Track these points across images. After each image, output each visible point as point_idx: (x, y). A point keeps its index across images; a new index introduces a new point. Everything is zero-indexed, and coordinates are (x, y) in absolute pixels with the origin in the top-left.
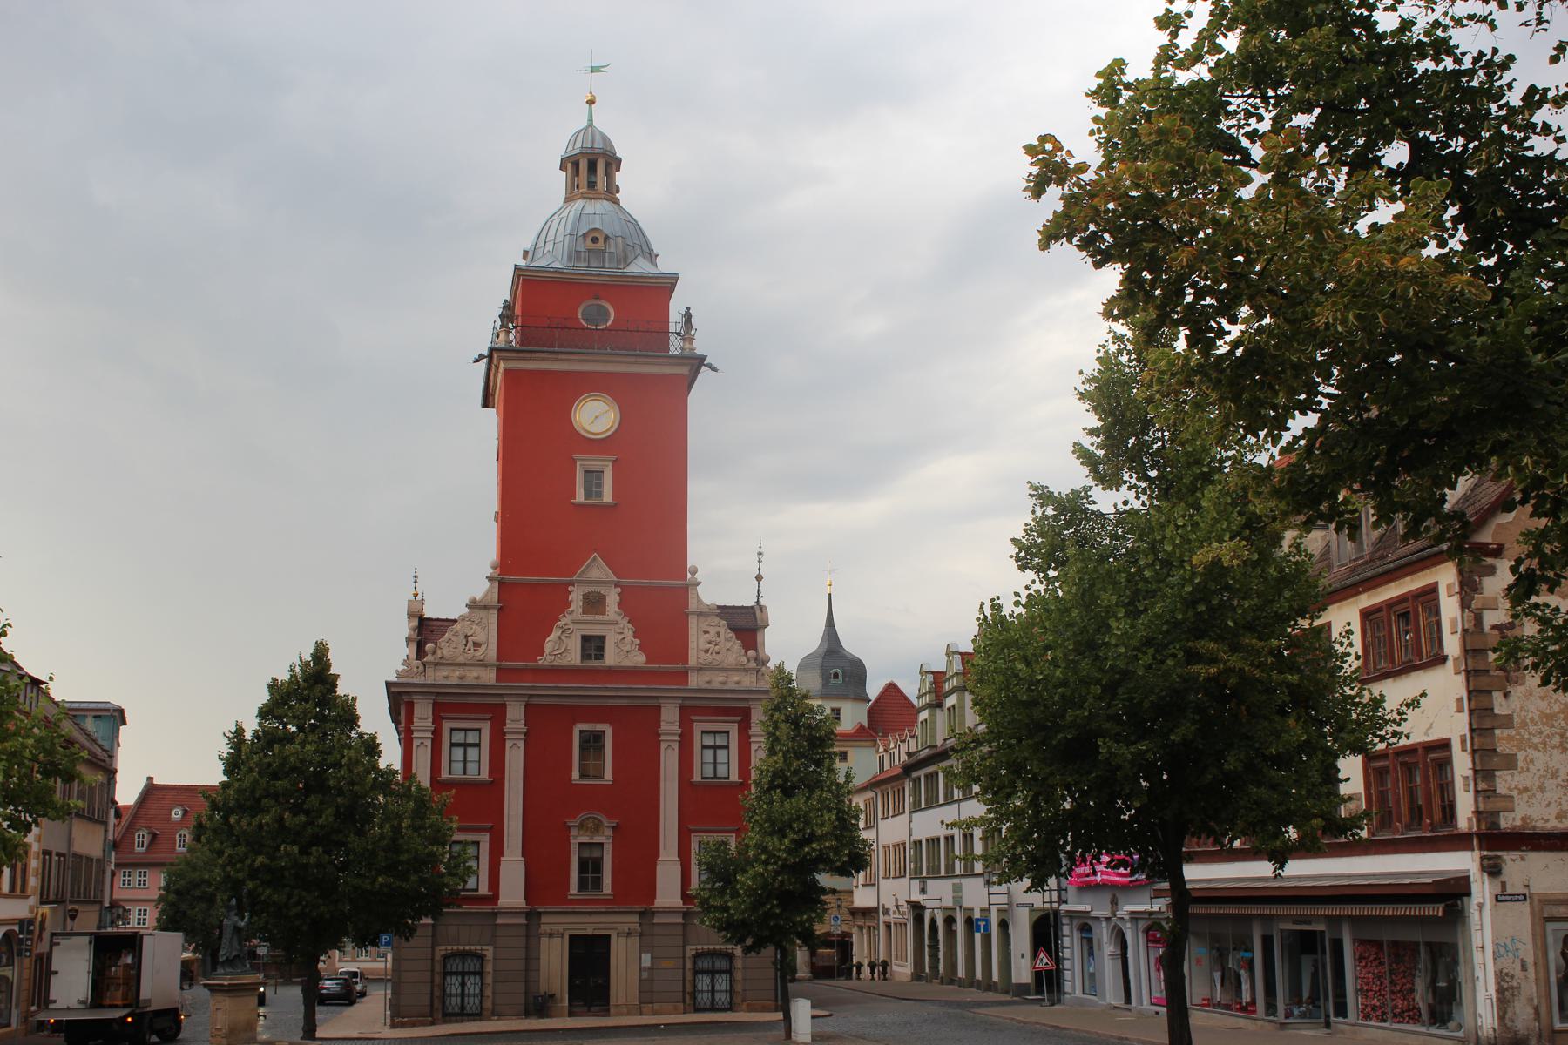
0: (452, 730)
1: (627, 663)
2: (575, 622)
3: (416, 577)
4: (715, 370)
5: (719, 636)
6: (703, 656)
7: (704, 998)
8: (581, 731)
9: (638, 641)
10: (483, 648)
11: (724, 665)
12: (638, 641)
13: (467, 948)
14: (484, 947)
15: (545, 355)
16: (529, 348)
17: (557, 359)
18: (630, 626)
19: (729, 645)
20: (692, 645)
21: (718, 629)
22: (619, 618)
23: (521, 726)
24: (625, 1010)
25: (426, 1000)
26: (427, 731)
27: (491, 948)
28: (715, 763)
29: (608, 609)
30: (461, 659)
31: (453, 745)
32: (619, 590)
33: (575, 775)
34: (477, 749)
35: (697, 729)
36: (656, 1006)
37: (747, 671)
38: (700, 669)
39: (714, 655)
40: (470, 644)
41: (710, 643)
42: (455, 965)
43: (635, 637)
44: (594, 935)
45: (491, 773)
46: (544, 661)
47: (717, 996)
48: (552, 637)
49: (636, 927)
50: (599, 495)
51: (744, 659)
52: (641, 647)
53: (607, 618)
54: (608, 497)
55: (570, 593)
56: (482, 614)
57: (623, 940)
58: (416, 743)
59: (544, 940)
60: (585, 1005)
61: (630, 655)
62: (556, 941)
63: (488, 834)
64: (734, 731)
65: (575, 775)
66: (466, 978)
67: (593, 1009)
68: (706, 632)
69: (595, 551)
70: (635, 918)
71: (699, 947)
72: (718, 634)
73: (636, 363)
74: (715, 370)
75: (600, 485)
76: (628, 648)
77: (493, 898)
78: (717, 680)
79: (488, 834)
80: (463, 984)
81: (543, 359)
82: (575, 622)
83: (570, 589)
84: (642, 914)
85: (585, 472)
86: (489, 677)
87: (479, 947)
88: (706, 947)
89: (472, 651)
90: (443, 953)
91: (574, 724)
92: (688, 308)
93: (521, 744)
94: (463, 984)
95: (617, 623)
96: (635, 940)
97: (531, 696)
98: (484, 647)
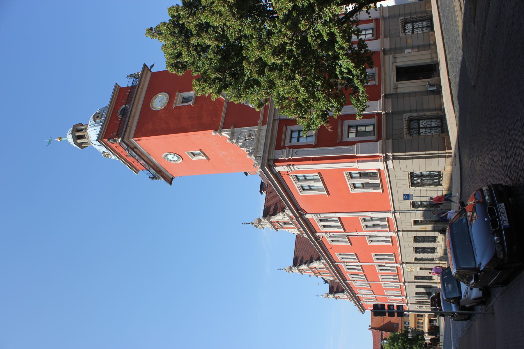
3: (244, 224)
4: (153, 65)
10: (252, 133)
14: (404, 117)
15: (130, 121)
16: (125, 126)
24: (434, 55)
26: (289, 151)
27: (405, 115)
44: (396, 72)
47: (433, 125)
49: (391, 56)
56: (236, 134)
57: (398, 60)
59: (399, 91)
62: (399, 86)
63: (344, 121)
66: (421, 126)
70: (387, 57)
73: (142, 89)
74: (153, 65)
77: (379, 115)
79: (344, 121)
81: (132, 123)
84: (385, 54)
86: (265, 127)
87: (404, 120)
92: (128, 76)
96: (397, 55)
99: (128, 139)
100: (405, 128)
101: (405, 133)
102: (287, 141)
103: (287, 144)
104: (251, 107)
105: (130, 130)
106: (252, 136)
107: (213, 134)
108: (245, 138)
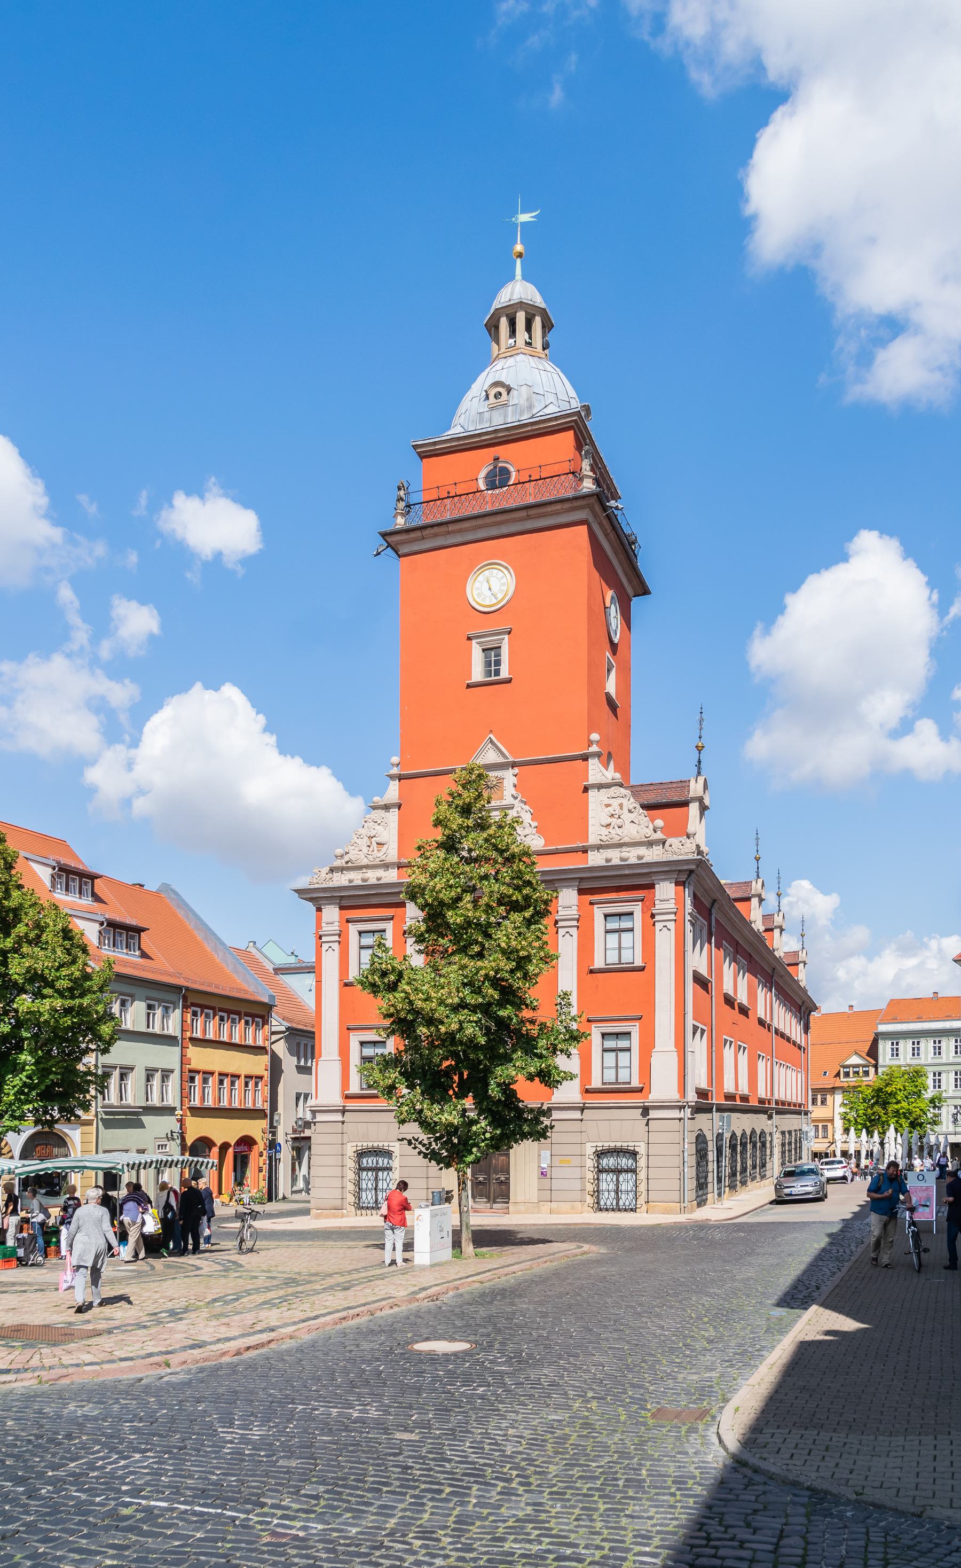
5: (621, 808)
6: (604, 831)
7: (608, 1199)
9: (535, 824)
11: (626, 840)
12: (535, 824)
13: (375, 1144)
14: (391, 1144)
18: (527, 808)
19: (632, 816)
20: (591, 822)
21: (620, 801)
22: (516, 802)
25: (337, 1193)
28: (620, 948)
30: (365, 862)
32: (516, 770)
35: (598, 913)
36: (554, 1205)
37: (650, 844)
38: (599, 847)
39: (619, 831)
41: (612, 815)
42: (368, 1161)
43: (532, 820)
50: (497, 673)
51: (649, 832)
53: (504, 803)
54: (505, 673)
58: (325, 946)
60: (489, 1201)
64: (637, 909)
67: (495, 1206)
68: (608, 806)
71: (600, 1144)
72: (621, 806)
75: (498, 663)
76: (527, 831)
78: (615, 856)
80: (376, 1179)
85: (484, 650)
87: (386, 1144)
88: (606, 1144)
90: (355, 1149)
94: (376, 1179)
100: (360, 1144)
101: (360, 1144)
103: (353, 929)
107: (395, 759)
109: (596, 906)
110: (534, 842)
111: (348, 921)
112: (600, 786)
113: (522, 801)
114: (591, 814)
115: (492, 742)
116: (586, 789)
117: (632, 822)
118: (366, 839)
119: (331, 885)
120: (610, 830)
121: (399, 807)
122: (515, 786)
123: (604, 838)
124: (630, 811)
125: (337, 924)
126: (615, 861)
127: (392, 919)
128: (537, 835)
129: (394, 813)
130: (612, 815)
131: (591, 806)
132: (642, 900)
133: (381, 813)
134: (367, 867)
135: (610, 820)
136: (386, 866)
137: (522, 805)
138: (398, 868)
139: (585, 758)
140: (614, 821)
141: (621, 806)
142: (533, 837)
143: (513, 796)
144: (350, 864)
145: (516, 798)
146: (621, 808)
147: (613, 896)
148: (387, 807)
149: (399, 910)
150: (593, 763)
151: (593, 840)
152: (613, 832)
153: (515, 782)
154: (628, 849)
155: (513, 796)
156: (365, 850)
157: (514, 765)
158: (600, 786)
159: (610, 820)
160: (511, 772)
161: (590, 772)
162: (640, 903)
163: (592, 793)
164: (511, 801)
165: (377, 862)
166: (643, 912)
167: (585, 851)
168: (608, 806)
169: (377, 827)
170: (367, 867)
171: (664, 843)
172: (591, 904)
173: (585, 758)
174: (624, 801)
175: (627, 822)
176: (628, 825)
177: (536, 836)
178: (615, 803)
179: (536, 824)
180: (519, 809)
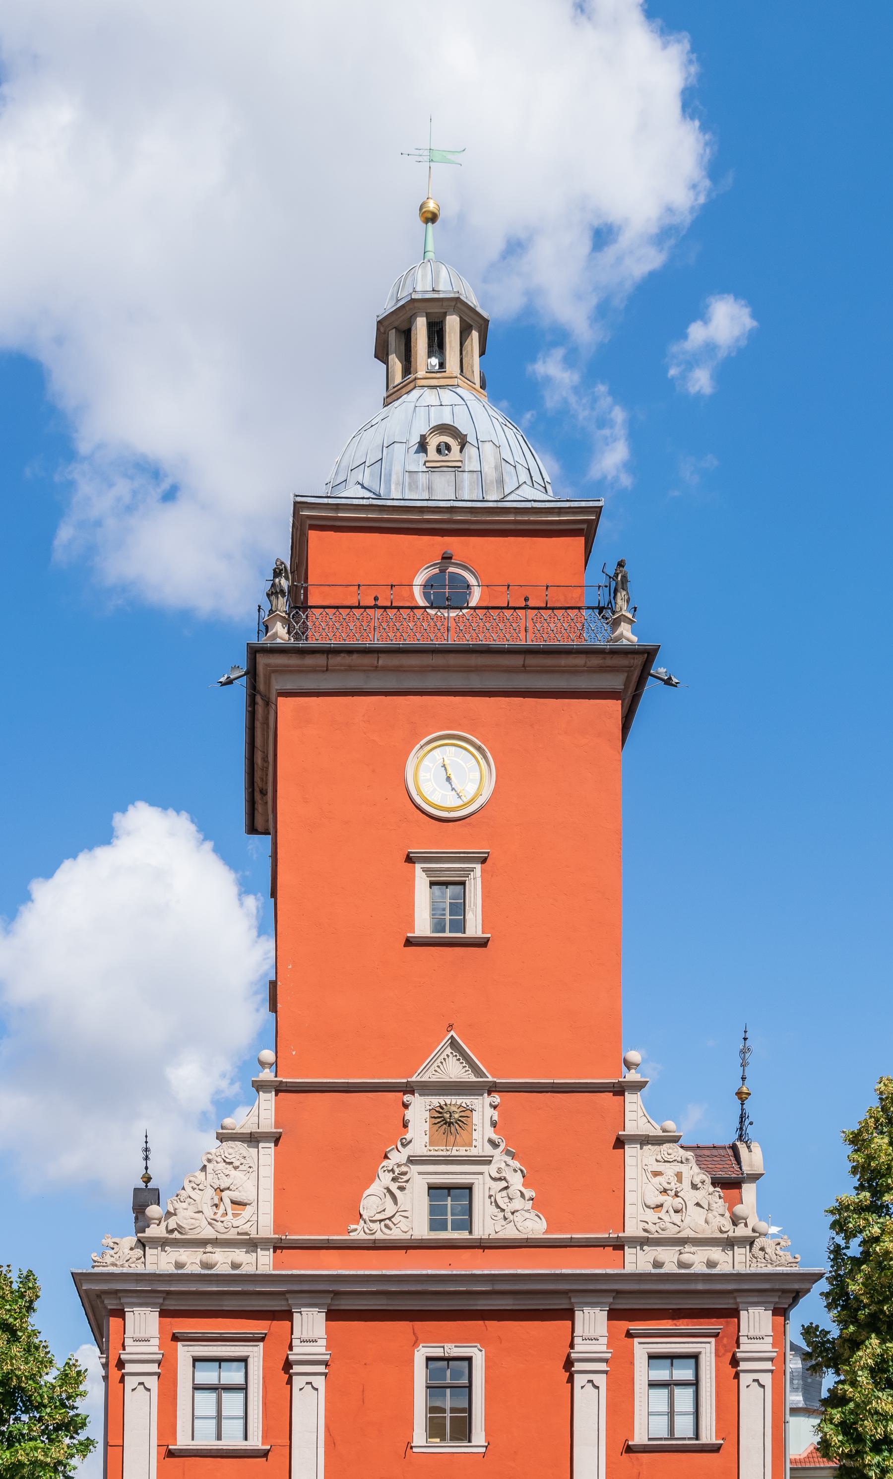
0: (196, 1360)
1: (509, 1232)
2: (411, 1161)
5: (680, 1180)
6: (651, 1216)
8: (429, 1359)
9: (529, 1193)
17: (376, 668)
18: (516, 1164)
19: (699, 1195)
20: (630, 1198)
21: (678, 1167)
23: (320, 1349)
29: (475, 1135)
30: (208, 1233)
31: (197, 1388)
32: (496, 1099)
33: (419, 1436)
34: (241, 1396)
35: (640, 1350)
38: (643, 1242)
39: (677, 1218)
40: (227, 1201)
41: (665, 1191)
45: (265, 1437)
46: (359, 1233)
48: (376, 1188)
51: (727, 1225)
52: (538, 1204)
53: (473, 1152)
54: (474, 928)
55: (406, 1106)
61: (518, 1217)
64: (707, 1350)
65: (419, 1436)
68: (656, 1174)
69: (451, 1026)
72: (679, 1176)
81: (351, 669)
82: (411, 1161)
83: (407, 1098)
89: (230, 1216)
91: (415, 1344)
93: (319, 1382)
95: (489, 1162)
97: (336, 1293)
98: (248, 1211)
99: (273, 672)
102: (196, 1348)
103: (185, 1353)
104: (364, 1196)
105: (314, 670)
106: (235, 1215)
108: (228, 1188)
109: (636, 1340)
110: (528, 1223)
111: (175, 1338)
112: (645, 1140)
113: (508, 1153)
114: (629, 1185)
115: (453, 1044)
116: (620, 1143)
117: (698, 1204)
118: (210, 1192)
119: (139, 1269)
120: (662, 1214)
121: (277, 1140)
122: (494, 1124)
123: (651, 1227)
124: (694, 1187)
125: (156, 1342)
126: (670, 1268)
127: (262, 1339)
128: (534, 1212)
129: (267, 1151)
130: (665, 1191)
131: (630, 1172)
132: (716, 1335)
133: (240, 1148)
134: (216, 1242)
135: (661, 1198)
136: (252, 1245)
137: (509, 1159)
138: (275, 1249)
139: (619, 1090)
140: (669, 1201)
141: (679, 1176)
142: (527, 1215)
143: (491, 1141)
144: (176, 1235)
145: (494, 1144)
146: (680, 1180)
147: (666, 1325)
148: (253, 1139)
149: (281, 1326)
150: (632, 1100)
151: (632, 1229)
152: (666, 1218)
153: (496, 1118)
154: (694, 1249)
155: (491, 1141)
156: (209, 1212)
157: (492, 1089)
158: (645, 1140)
159: (661, 1198)
160: (487, 1099)
161: (628, 1116)
162: (713, 1340)
163: (631, 1151)
164: (489, 1150)
165: (232, 1235)
166: (717, 1355)
167: (619, 1245)
168: (656, 1174)
169: (233, 1173)
170: (216, 1242)
171: (752, 1244)
172: (629, 1335)
173: (619, 1090)
174: (683, 1168)
175: (690, 1205)
176: (692, 1209)
177: (532, 1215)
178: (670, 1170)
179: (533, 1194)
180: (503, 1165)
